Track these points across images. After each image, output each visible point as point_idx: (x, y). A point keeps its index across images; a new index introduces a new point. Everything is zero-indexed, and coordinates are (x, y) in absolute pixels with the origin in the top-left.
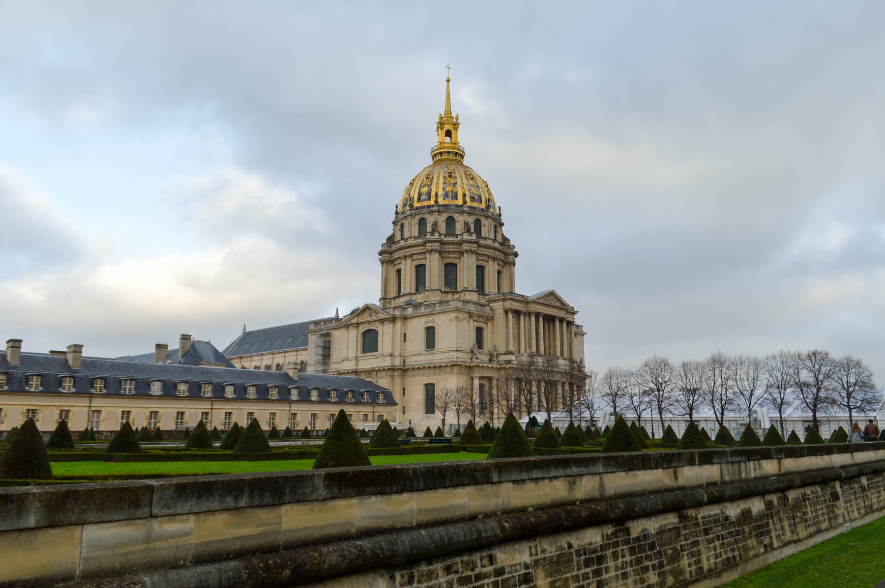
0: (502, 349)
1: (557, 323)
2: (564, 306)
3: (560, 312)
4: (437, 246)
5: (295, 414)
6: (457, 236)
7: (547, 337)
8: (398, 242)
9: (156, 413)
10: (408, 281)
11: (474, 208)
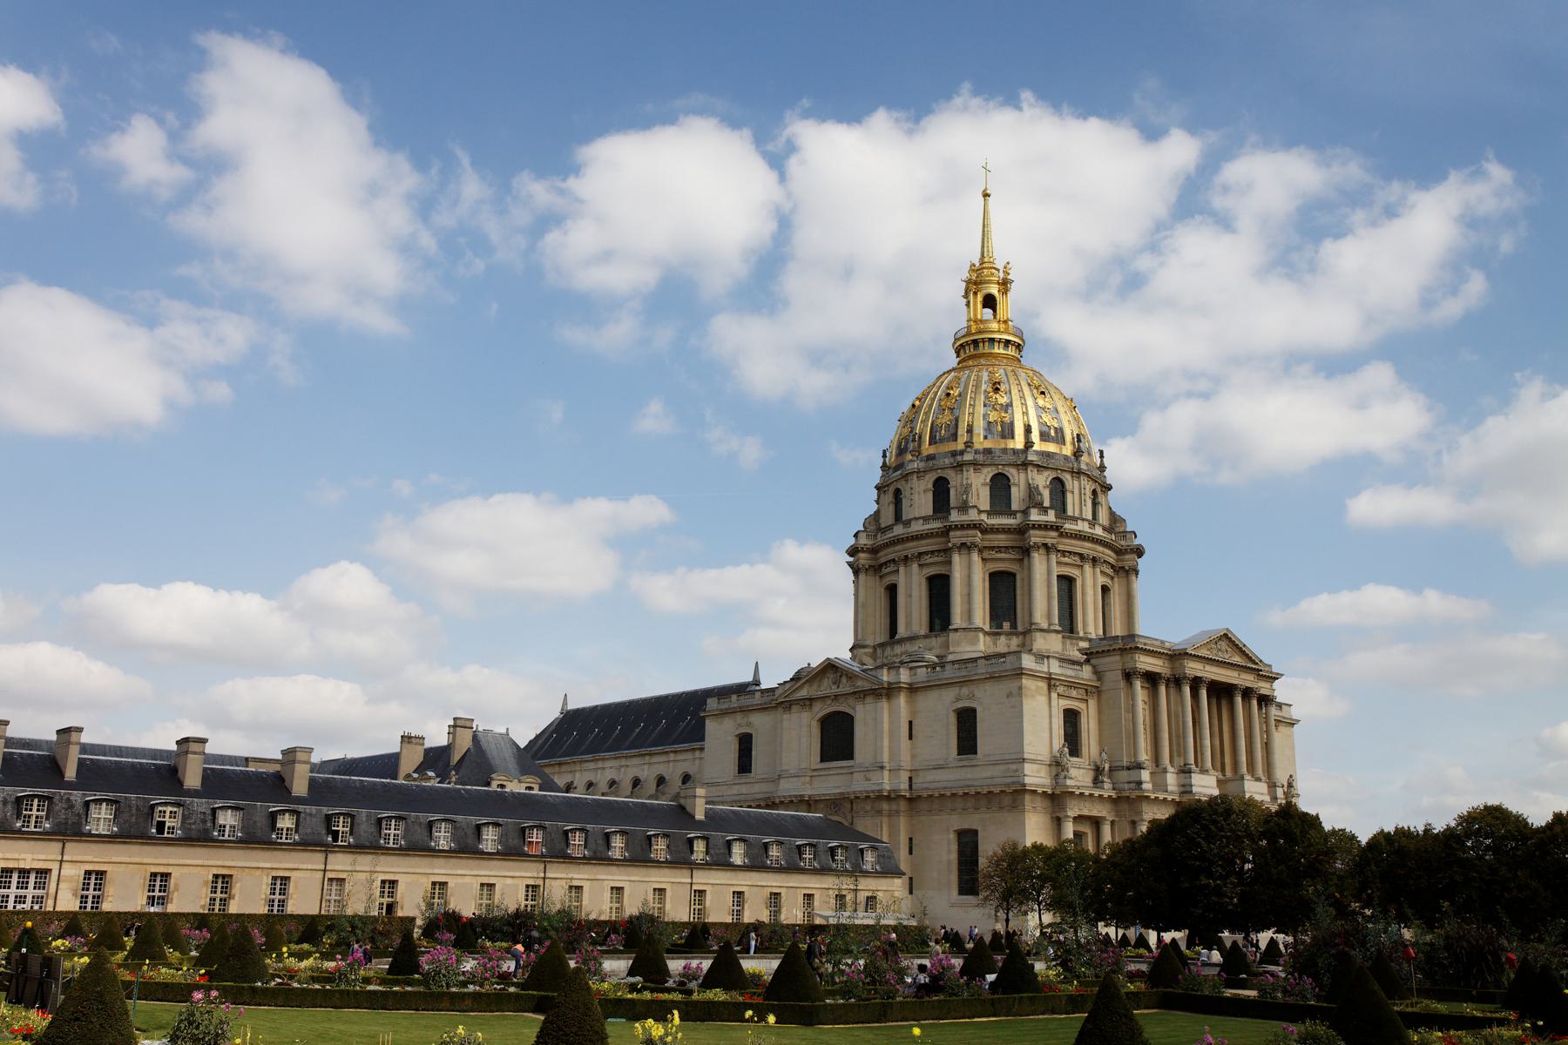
1: (1239, 700)
2: (1252, 665)
3: (1244, 676)
4: (978, 537)
5: (701, 893)
6: (1013, 514)
8: (890, 528)
9: (443, 884)
11: (1048, 455)
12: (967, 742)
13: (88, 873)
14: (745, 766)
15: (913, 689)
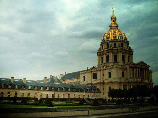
0: (129, 77)
4: (112, 50)
6: (117, 48)
7: (142, 73)
9: (42, 94)
10: (104, 60)
12: (110, 76)
13: (1, 92)
14: (84, 80)
15: (103, 70)
